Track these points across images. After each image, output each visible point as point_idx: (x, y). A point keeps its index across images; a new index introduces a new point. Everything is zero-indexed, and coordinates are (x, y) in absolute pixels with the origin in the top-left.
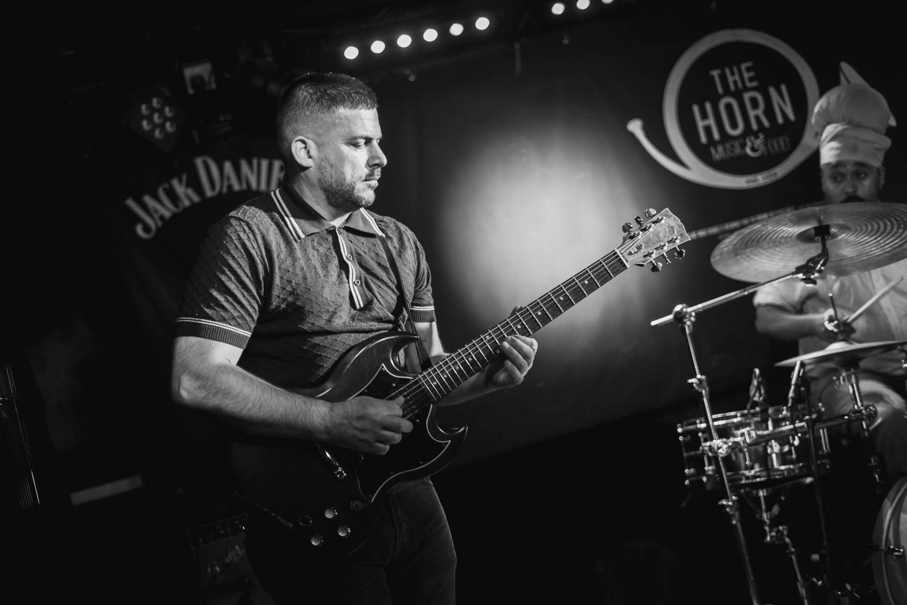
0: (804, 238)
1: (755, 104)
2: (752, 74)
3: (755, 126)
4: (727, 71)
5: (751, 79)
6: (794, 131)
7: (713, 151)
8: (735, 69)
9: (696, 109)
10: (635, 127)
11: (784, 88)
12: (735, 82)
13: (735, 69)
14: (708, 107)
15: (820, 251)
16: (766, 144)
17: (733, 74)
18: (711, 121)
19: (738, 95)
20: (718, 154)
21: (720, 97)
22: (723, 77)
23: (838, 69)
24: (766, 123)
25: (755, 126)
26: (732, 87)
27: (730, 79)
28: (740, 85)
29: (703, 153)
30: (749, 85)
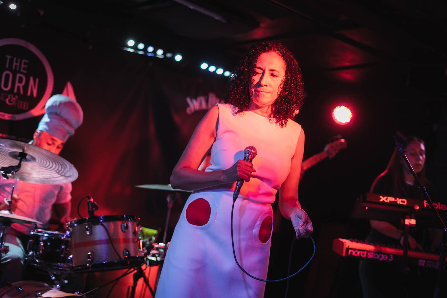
0: (13, 155)
1: (20, 81)
2: (26, 66)
3: (16, 91)
4: (15, 59)
5: (24, 69)
8: (19, 60)
11: (37, 81)
12: (16, 66)
13: (19, 60)
15: (17, 165)
17: (17, 62)
19: (15, 73)
22: (11, 61)
24: (22, 92)
25: (16, 91)
26: (14, 68)
27: (15, 64)
28: (18, 69)
30: (22, 70)
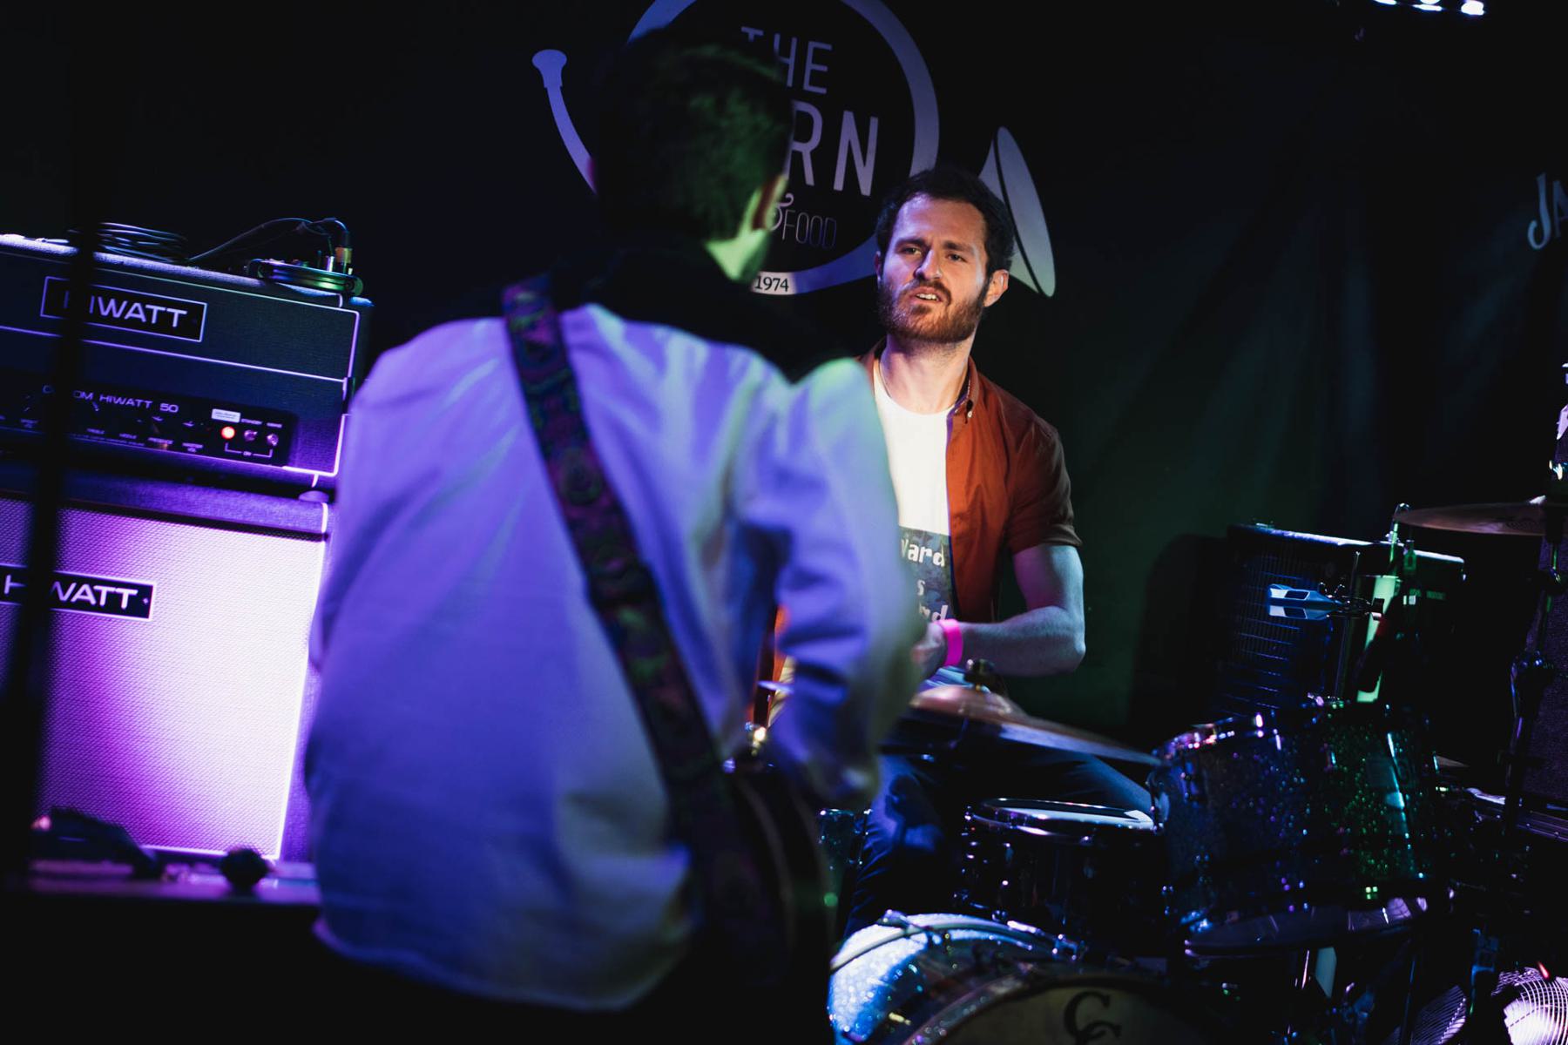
5: (816, 79)
16: (792, 219)
30: (807, 87)
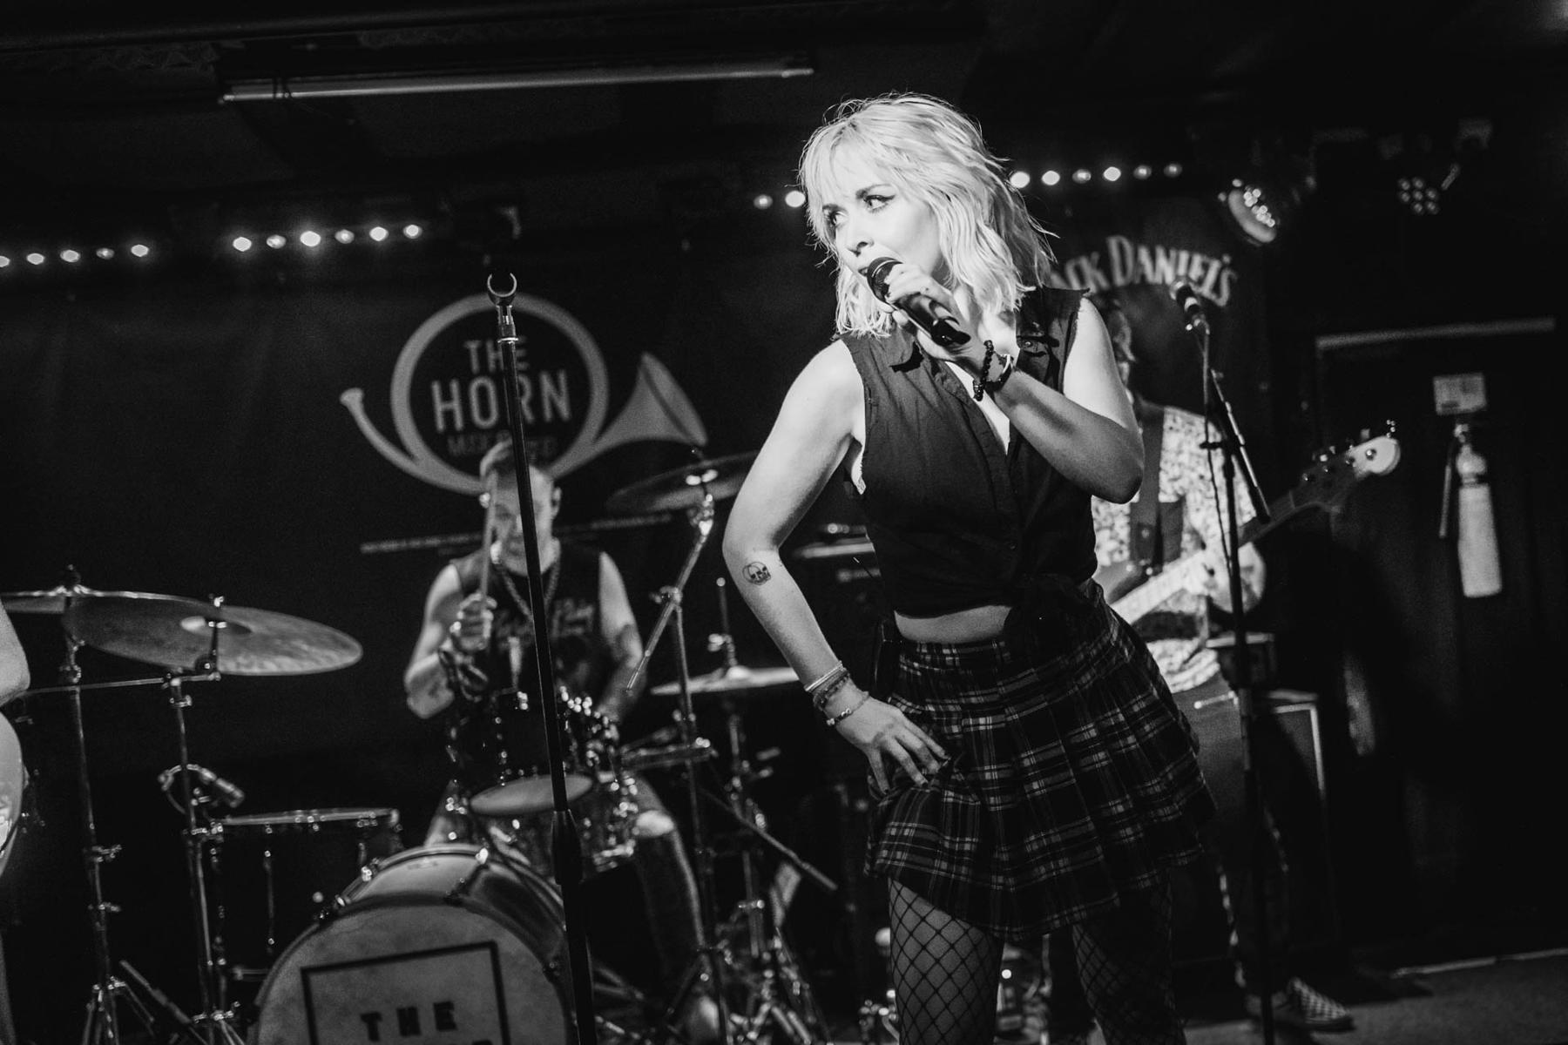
4: (489, 345)
5: (520, 360)
6: (563, 433)
7: (451, 441)
9: (436, 388)
10: (353, 399)
11: (562, 377)
12: (497, 361)
14: (455, 387)
18: (455, 405)
20: (458, 447)
21: (472, 377)
22: (482, 353)
23: (636, 363)
29: (437, 443)
